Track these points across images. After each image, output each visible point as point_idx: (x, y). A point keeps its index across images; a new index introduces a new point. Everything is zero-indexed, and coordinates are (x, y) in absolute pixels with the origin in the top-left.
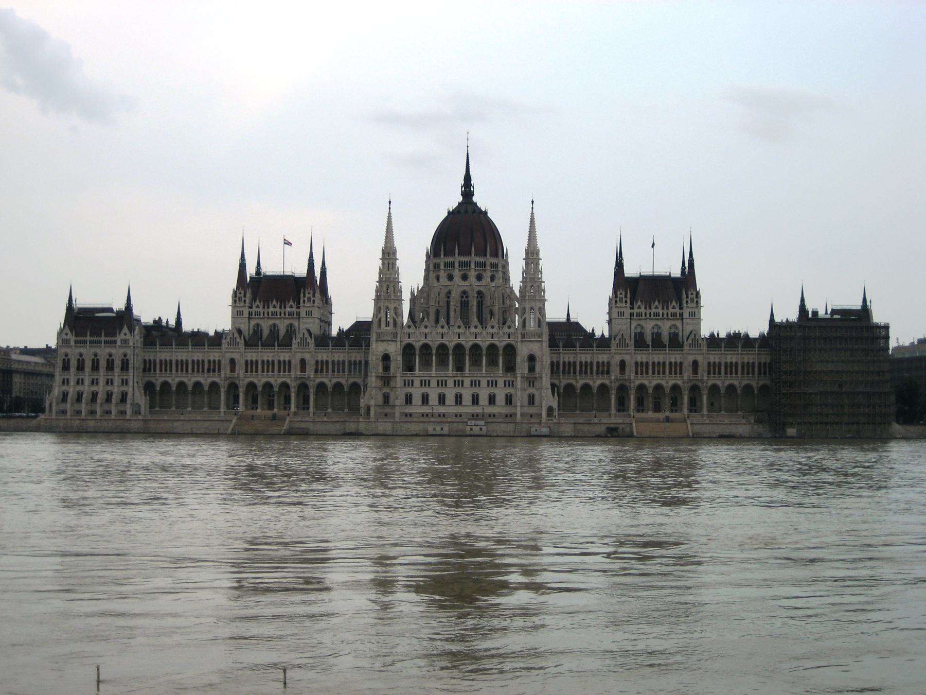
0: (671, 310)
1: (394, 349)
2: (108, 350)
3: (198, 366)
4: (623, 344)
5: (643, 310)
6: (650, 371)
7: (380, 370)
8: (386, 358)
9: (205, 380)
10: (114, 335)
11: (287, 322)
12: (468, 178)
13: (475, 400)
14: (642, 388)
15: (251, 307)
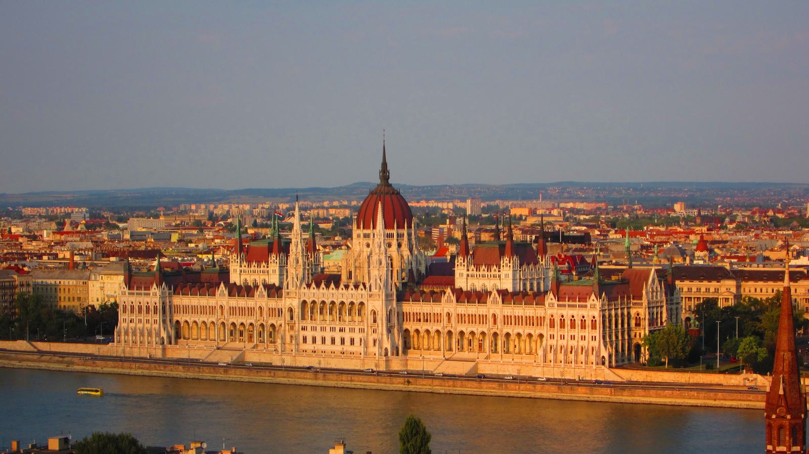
0: (493, 273)
1: (295, 304)
2: (147, 299)
3: (203, 310)
4: (449, 301)
5: (475, 272)
6: (467, 321)
7: (288, 317)
8: (291, 310)
9: (209, 319)
10: (147, 288)
11: (262, 277)
12: (384, 165)
13: (343, 341)
14: (462, 333)
15: (241, 266)
